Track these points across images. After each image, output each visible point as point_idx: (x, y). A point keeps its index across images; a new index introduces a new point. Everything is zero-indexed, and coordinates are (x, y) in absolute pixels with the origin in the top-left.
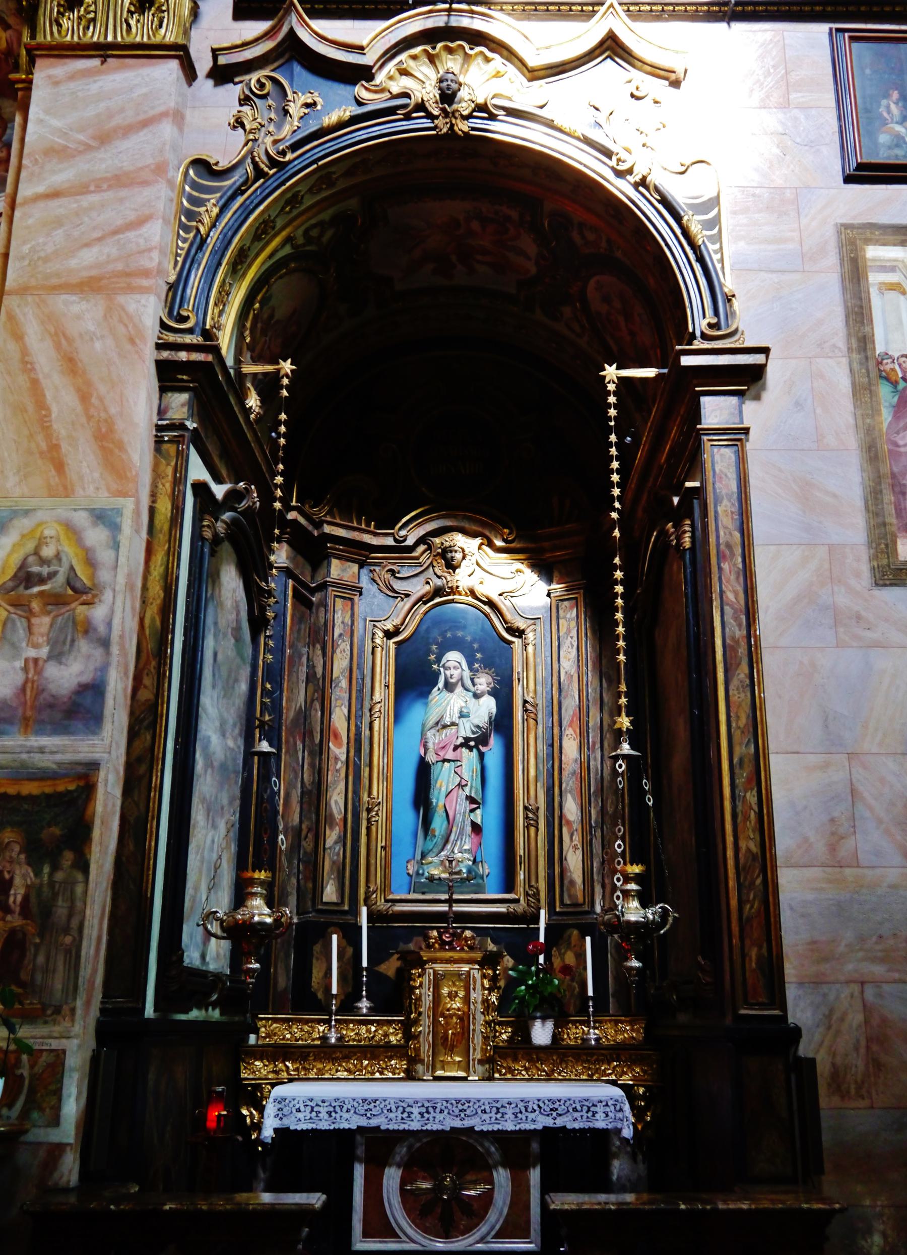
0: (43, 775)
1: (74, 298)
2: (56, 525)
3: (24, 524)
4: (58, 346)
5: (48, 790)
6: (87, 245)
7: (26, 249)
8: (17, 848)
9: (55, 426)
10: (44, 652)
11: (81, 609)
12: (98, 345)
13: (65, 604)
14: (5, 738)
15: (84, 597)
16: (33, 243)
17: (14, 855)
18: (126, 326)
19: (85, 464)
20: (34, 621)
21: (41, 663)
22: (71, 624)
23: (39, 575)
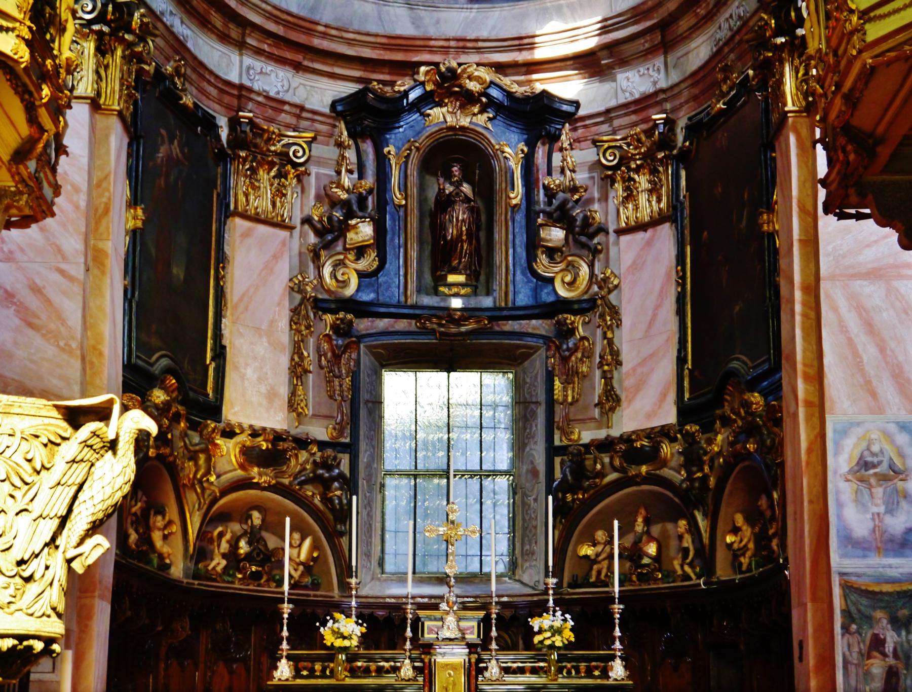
0: (892, 581)
1: (865, 283)
2: (878, 432)
3: (857, 431)
4: (860, 315)
5: (898, 589)
6: (868, 246)
7: (830, 248)
8: (885, 621)
9: (867, 369)
10: (882, 509)
11: (900, 484)
12: (885, 315)
13: (890, 480)
14: (869, 559)
15: (901, 476)
16: (834, 244)
17: (884, 625)
18: (901, 302)
19: (889, 393)
20: (873, 490)
21: (881, 516)
22: (895, 492)
23: (872, 463)
